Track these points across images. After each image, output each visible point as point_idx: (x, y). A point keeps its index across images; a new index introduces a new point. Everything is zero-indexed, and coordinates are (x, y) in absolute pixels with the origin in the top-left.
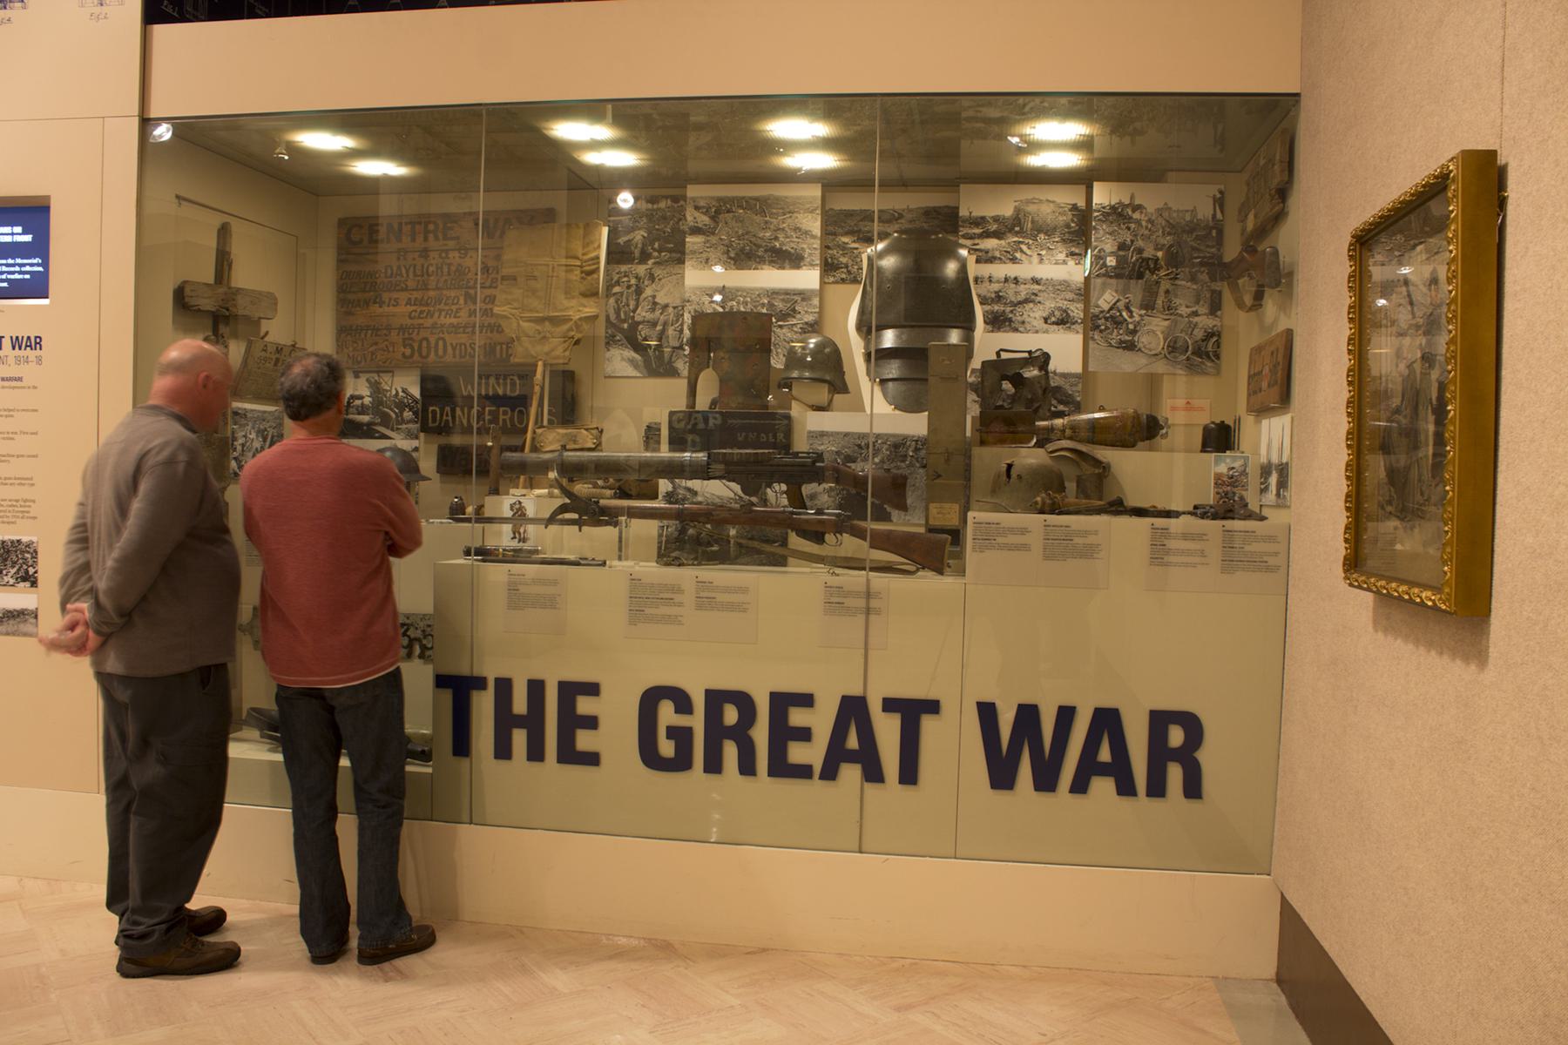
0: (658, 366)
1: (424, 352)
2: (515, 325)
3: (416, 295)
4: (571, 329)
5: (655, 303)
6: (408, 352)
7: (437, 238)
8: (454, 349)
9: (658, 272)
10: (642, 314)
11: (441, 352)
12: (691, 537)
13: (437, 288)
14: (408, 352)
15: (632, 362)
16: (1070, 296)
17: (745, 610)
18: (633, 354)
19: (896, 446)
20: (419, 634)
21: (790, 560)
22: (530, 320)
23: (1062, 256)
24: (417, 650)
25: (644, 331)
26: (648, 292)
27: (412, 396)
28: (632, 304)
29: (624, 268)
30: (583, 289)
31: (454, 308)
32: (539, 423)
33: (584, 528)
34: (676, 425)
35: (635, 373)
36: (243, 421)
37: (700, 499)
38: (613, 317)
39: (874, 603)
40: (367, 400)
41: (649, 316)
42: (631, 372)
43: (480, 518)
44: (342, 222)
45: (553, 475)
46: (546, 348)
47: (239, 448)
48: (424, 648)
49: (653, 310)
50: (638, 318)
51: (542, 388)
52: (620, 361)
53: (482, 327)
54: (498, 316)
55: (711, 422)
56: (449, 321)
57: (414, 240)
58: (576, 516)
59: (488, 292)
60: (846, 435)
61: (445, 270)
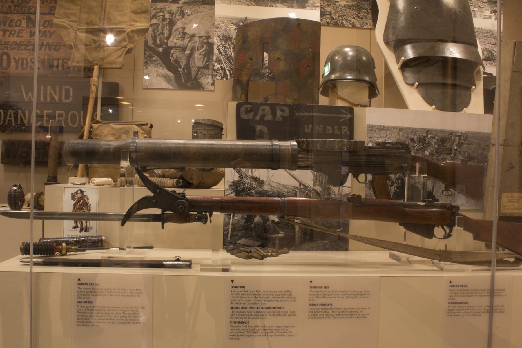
0: (187, 79)
2: (72, 35)
5: (184, 34)
8: (17, 63)
9: (188, 11)
10: (174, 41)
12: (258, 224)
15: (166, 78)
16: (493, 41)
17: (365, 316)
18: (166, 72)
19: (443, 141)
21: (352, 243)
23: (488, 13)
25: (175, 54)
26: (179, 24)
28: (166, 33)
29: (160, 5)
30: (134, 7)
31: (17, 29)
32: (94, 120)
33: (166, 225)
34: (243, 116)
35: (168, 86)
37: (266, 188)
38: (150, 42)
39: (498, 301)
41: (180, 43)
42: (164, 84)
43: (40, 211)
45: (125, 164)
49: (183, 38)
50: (170, 44)
51: (97, 88)
52: (153, 76)
53: (41, 45)
54: (57, 25)
55: (279, 113)
58: (158, 211)
59: (47, 17)
60: (401, 129)
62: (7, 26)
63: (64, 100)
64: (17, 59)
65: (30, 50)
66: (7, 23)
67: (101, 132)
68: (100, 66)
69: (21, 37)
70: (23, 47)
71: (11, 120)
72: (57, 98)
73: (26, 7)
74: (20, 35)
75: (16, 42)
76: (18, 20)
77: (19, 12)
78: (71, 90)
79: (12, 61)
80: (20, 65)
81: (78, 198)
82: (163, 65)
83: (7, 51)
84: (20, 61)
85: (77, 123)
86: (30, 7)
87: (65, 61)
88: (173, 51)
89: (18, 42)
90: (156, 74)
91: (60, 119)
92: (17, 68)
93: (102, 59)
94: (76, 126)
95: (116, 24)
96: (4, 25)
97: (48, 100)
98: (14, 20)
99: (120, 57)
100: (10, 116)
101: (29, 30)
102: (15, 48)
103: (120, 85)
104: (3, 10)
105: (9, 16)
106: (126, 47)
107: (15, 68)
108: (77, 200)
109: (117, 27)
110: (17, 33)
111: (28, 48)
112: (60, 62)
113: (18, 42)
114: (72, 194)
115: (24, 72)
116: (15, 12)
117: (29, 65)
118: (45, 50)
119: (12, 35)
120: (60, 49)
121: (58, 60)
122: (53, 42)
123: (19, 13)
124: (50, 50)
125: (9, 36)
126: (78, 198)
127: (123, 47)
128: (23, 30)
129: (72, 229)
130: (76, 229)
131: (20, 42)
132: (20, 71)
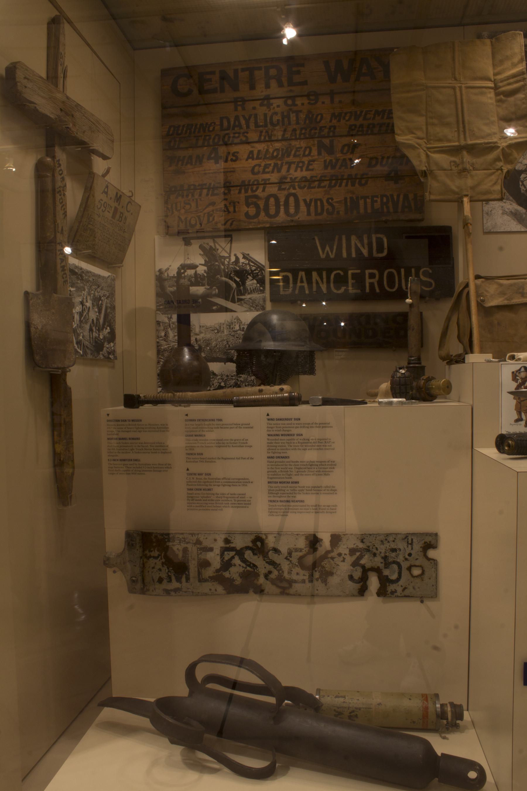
1: (272, 211)
3: (261, 147)
4: (498, 159)
6: (252, 211)
7: (280, 85)
8: (308, 206)
11: (292, 210)
13: (284, 139)
14: (252, 211)
15: (515, 215)
20: (378, 562)
22: (442, 151)
24: (374, 582)
27: (255, 263)
31: (306, 160)
36: (80, 284)
40: (201, 270)
44: (165, 73)
46: (470, 182)
47: (77, 317)
48: (384, 581)
56: (299, 174)
57: (252, 87)
61: (293, 117)
62: (291, 157)
63: (375, 254)
64: (308, 200)
65: (324, 187)
66: (293, 152)
67: (486, 291)
68: (471, 197)
69: (312, 170)
70: (316, 183)
71: (303, 287)
72: (365, 252)
73: (316, 129)
74: (311, 167)
75: (306, 177)
76: (306, 148)
77: (307, 136)
78: (385, 240)
79: (302, 204)
80: (312, 208)
81: (522, 379)
82: (511, 198)
83: (293, 191)
84: (313, 204)
85: (397, 285)
86: (321, 128)
87: (375, 199)
88: (523, 176)
89: (309, 177)
90: (501, 212)
91: (372, 281)
92: (309, 214)
93: (473, 188)
94: (394, 290)
95: (483, 138)
96: (289, 156)
97: (354, 255)
98: (301, 148)
99: (495, 184)
100: (302, 282)
101: (323, 160)
102: (305, 186)
103: (453, 228)
104: (286, 136)
105: (293, 143)
106: (502, 170)
107: (306, 214)
108: (520, 381)
109: (486, 141)
110: (306, 166)
111: (322, 185)
112: (369, 201)
113: (309, 177)
114: (513, 373)
115: (319, 217)
116: (302, 136)
117: (325, 208)
118: (346, 185)
119: (299, 169)
120: (366, 183)
121: (365, 198)
122: (356, 175)
123: (307, 138)
124: (353, 185)
125: (296, 171)
126: (522, 379)
127: (498, 170)
128: (314, 161)
129: (513, 423)
130: (520, 422)
131: (312, 177)
132: (313, 217)
